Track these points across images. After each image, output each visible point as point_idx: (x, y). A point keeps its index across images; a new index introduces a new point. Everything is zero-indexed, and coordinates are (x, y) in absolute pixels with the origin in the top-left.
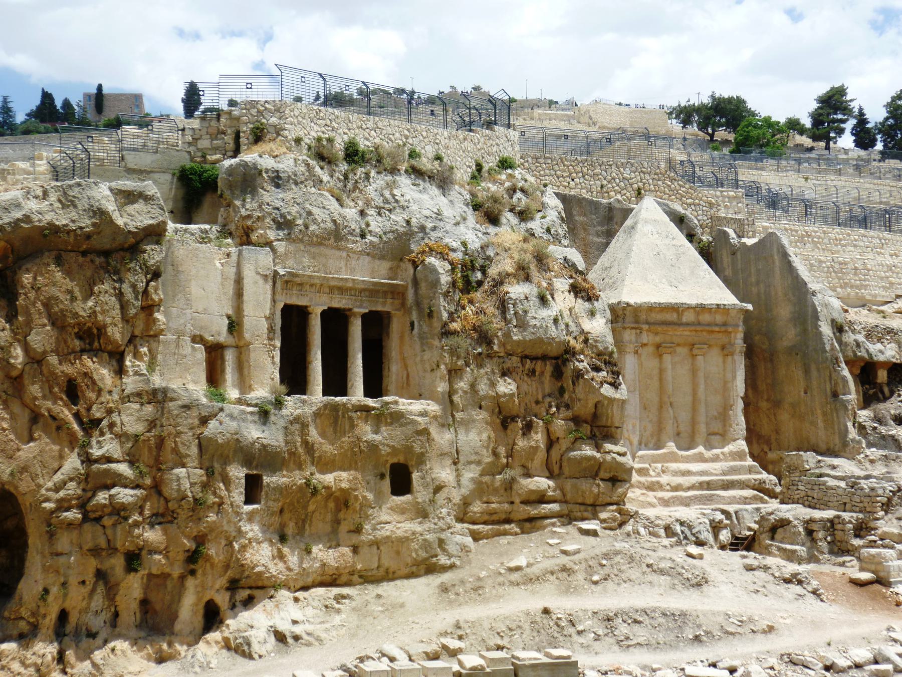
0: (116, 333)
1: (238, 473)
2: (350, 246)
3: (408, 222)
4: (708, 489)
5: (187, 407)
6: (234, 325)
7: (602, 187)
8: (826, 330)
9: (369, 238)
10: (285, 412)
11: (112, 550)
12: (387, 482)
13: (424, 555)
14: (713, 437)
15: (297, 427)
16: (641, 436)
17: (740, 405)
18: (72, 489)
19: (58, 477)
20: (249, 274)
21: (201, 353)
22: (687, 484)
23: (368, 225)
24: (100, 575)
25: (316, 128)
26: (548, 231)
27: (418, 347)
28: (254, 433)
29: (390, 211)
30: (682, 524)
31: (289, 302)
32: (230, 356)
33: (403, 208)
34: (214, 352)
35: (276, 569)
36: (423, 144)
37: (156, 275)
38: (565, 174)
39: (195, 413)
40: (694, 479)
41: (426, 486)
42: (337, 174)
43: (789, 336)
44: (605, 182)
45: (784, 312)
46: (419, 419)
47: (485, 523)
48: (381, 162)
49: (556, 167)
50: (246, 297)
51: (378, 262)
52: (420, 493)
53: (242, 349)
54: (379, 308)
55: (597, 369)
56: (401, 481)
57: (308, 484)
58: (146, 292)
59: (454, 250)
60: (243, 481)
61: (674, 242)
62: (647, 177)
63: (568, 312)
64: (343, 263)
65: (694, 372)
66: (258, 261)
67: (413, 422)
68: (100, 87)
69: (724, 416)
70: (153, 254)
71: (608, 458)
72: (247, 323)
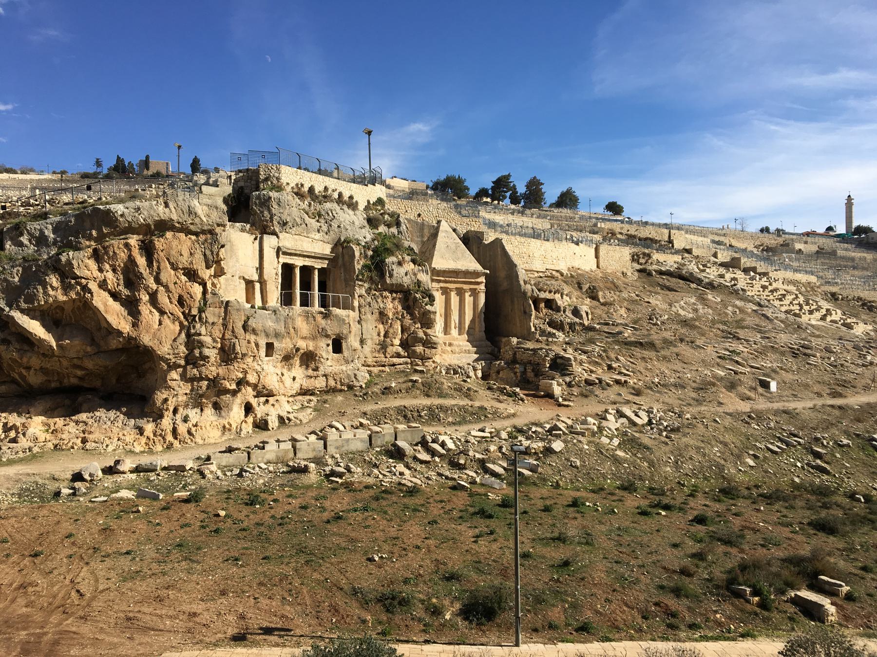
1: (263, 342)
3: (339, 227)
5: (238, 310)
8: (522, 283)
11: (201, 379)
12: (331, 347)
13: (347, 381)
21: (243, 285)
27: (344, 286)
30: (460, 368)
32: (257, 286)
34: (249, 284)
37: (223, 246)
41: (348, 349)
43: (505, 285)
45: (502, 274)
47: (374, 366)
48: (326, 197)
50: (265, 259)
52: (346, 353)
53: (262, 282)
56: (337, 347)
58: (218, 254)
66: (270, 242)
67: (344, 320)
68: (147, 157)
72: (265, 271)
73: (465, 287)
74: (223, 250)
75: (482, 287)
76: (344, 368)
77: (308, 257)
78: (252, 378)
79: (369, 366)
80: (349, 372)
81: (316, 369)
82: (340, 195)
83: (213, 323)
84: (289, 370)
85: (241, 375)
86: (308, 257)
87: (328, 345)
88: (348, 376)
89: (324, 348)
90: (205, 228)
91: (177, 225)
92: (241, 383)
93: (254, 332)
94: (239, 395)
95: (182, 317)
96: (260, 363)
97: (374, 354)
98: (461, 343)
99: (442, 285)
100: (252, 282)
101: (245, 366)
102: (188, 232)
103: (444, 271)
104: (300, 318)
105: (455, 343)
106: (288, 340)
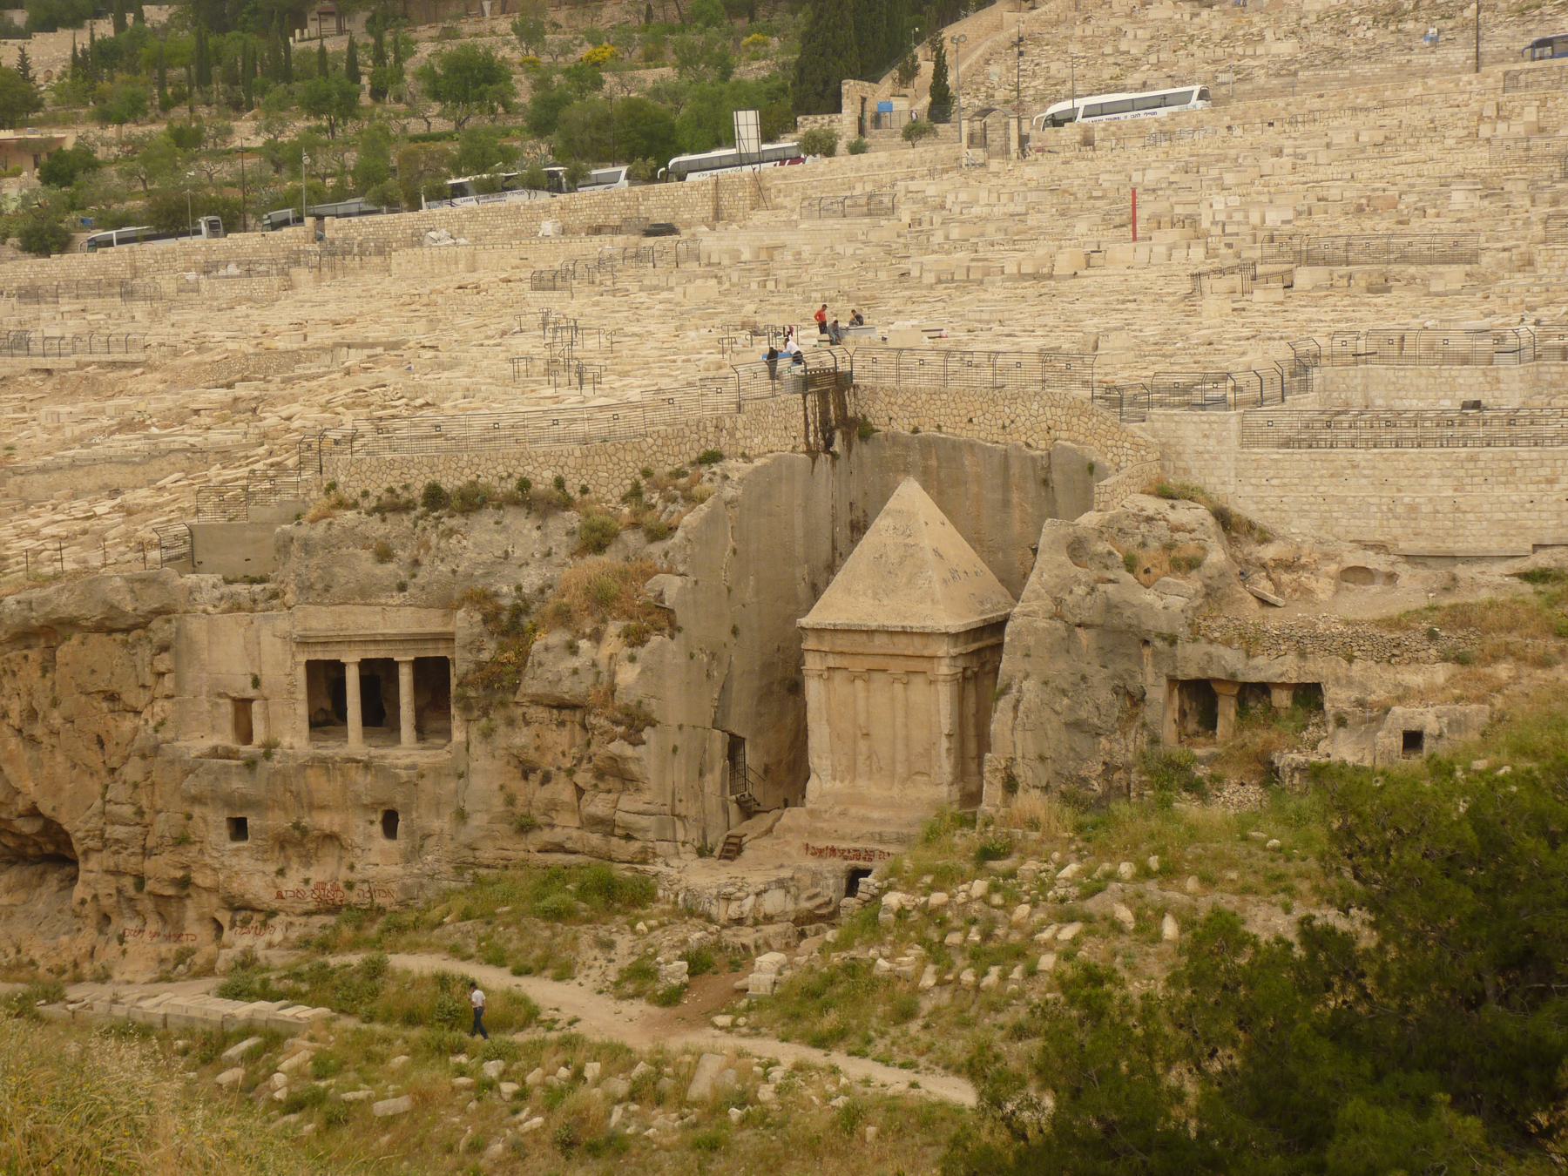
0: (131, 697)
2: (383, 601)
3: (454, 572)
4: (881, 841)
5: (172, 762)
6: (256, 683)
7: (1004, 427)
9: (411, 590)
10: (269, 764)
12: (378, 828)
13: (402, 897)
14: (918, 778)
15: (279, 778)
16: (834, 769)
17: (945, 744)
18: (96, 822)
19: (89, 813)
20: (266, 637)
21: (227, 707)
22: (856, 834)
23: (414, 576)
24: (119, 891)
25: (390, 478)
26: (666, 555)
28: (238, 785)
29: (442, 560)
31: (313, 658)
32: (256, 707)
33: (455, 556)
35: (267, 897)
36: (538, 471)
37: (164, 648)
38: (963, 412)
39: (177, 767)
40: (866, 829)
41: (410, 833)
42: (406, 523)
44: (1007, 422)
46: (403, 773)
49: (952, 405)
51: (423, 613)
52: (401, 842)
54: (432, 654)
55: (617, 723)
57: (296, 826)
59: (505, 596)
60: (225, 824)
61: (910, 541)
62: (1059, 411)
63: (606, 661)
64: (378, 618)
65: (893, 699)
67: (396, 776)
69: (928, 753)
70: (161, 630)
71: (619, 816)
73: (897, 667)
74: (165, 656)
75: (944, 669)
76: (397, 870)
77: (375, 642)
78: (199, 878)
79: (488, 867)
80: (409, 881)
81: (352, 868)
82: (524, 484)
83: (136, 786)
84: (307, 864)
85: (179, 874)
86: (375, 642)
87: (372, 822)
88: (405, 889)
89: (364, 831)
90: (131, 621)
91: (84, 623)
92: (185, 883)
93: (196, 800)
94: (188, 902)
95: (103, 773)
96: (215, 854)
97: (499, 844)
98: (876, 815)
99: (832, 661)
100: (250, 701)
101: (183, 860)
102: (110, 631)
103: (835, 631)
104: (309, 771)
105: (853, 811)
106: (278, 813)
